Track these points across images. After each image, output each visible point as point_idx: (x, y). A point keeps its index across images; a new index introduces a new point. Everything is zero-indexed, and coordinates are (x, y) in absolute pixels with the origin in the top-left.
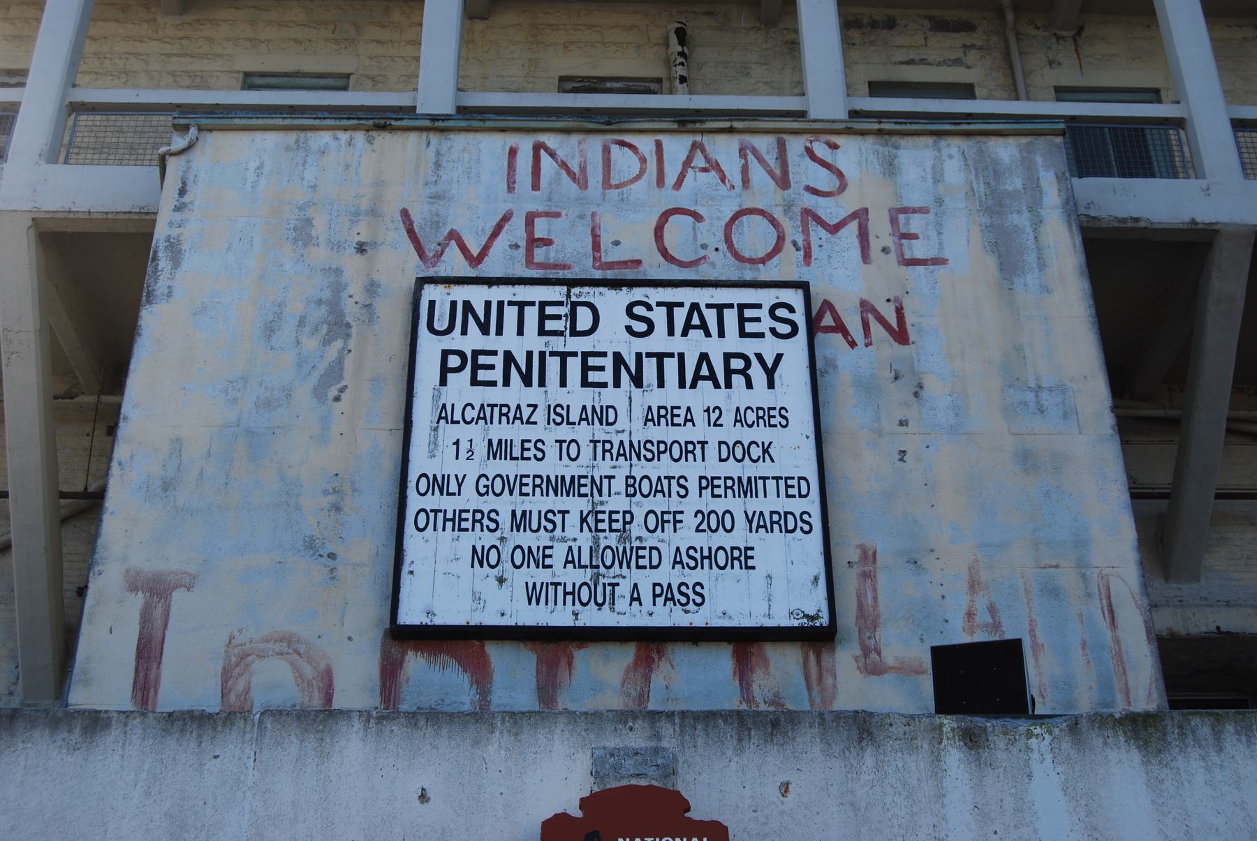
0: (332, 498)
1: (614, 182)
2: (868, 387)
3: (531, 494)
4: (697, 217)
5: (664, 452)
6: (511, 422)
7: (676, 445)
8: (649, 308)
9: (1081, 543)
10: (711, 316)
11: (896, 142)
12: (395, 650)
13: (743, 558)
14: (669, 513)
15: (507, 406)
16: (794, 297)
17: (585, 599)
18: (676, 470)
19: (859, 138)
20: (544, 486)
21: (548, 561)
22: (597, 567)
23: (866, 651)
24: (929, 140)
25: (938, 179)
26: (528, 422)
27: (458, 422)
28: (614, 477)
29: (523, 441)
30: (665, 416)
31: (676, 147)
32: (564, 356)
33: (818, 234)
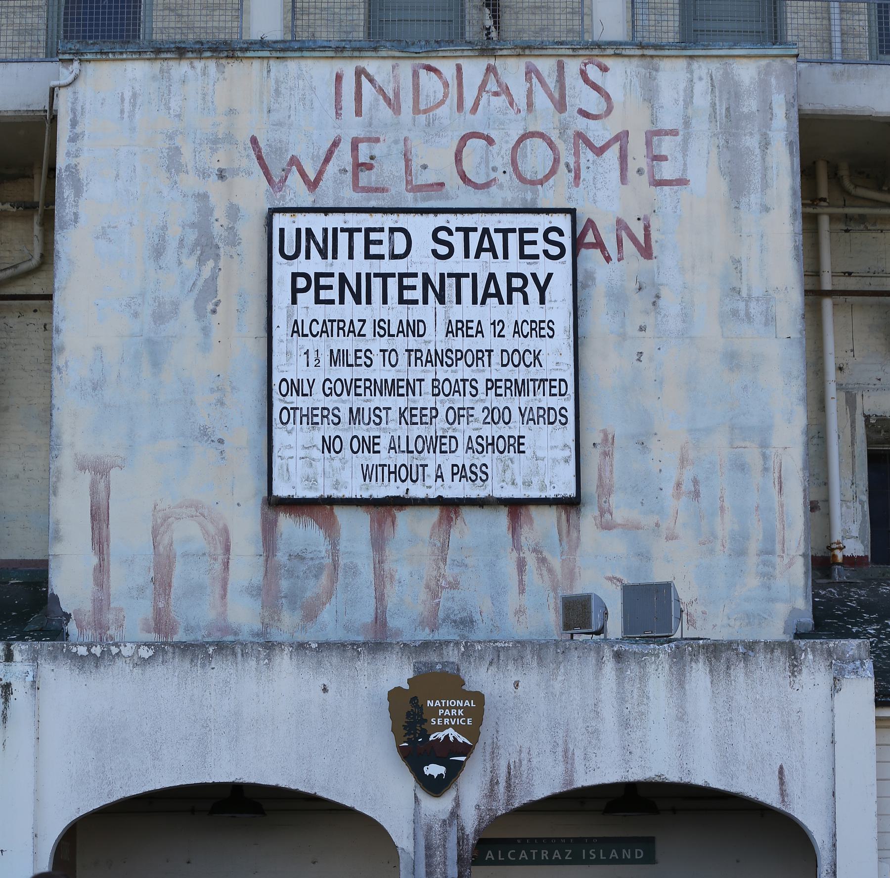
0: (217, 395)
1: (422, 107)
2: (617, 297)
3: (363, 395)
4: (490, 141)
5: (460, 359)
6: (346, 335)
8: (450, 233)
10: (498, 239)
11: (657, 64)
12: (271, 514)
13: (517, 444)
14: (464, 409)
15: (343, 321)
16: (563, 222)
18: (468, 374)
19: (626, 60)
20: (372, 388)
21: (377, 448)
22: (412, 452)
23: (602, 513)
26: (359, 335)
27: (307, 335)
28: (423, 380)
29: (356, 351)
30: (461, 329)
32: (385, 277)
33: (587, 155)
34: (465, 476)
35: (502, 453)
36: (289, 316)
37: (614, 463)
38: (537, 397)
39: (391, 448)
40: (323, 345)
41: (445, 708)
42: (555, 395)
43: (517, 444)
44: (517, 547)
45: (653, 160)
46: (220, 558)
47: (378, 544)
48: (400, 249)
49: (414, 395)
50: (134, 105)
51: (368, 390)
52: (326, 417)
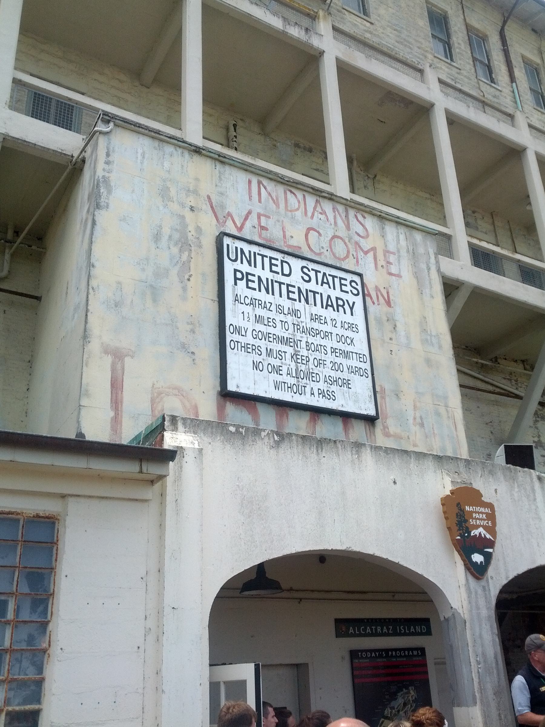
0: (191, 327)
2: (379, 321)
4: (320, 234)
5: (318, 334)
8: (309, 271)
9: (446, 398)
10: (330, 279)
13: (346, 383)
16: (357, 279)
18: (323, 342)
21: (281, 372)
24: (394, 225)
26: (269, 310)
27: (243, 304)
30: (317, 319)
31: (311, 201)
33: (361, 254)
36: (234, 292)
41: (476, 512)
43: (346, 383)
50: (144, 157)
52: (254, 350)
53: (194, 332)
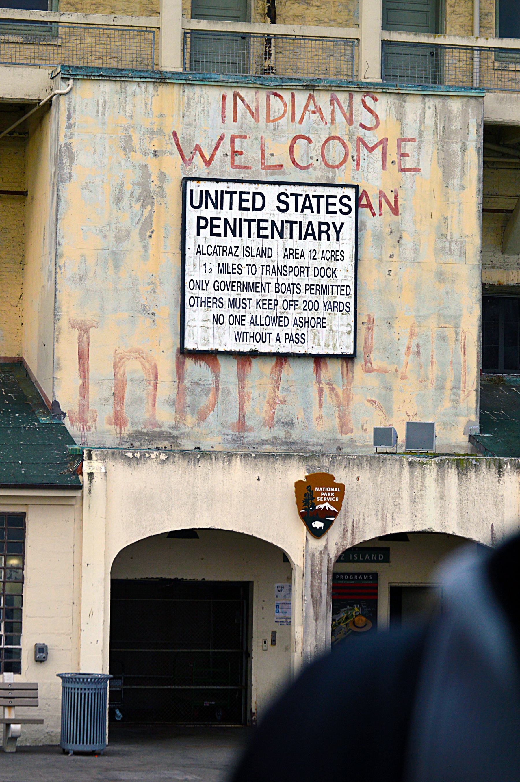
0: (151, 287)
2: (378, 237)
4: (309, 141)
5: (291, 272)
7: (296, 268)
8: (287, 197)
10: (314, 201)
12: (181, 357)
13: (321, 322)
14: (292, 301)
15: (226, 247)
16: (351, 192)
17: (258, 340)
18: (295, 280)
19: (388, 95)
20: (242, 287)
21: (243, 322)
22: (263, 325)
25: (422, 121)
26: (235, 255)
27: (205, 254)
28: (270, 283)
30: (292, 254)
31: (301, 98)
32: (250, 221)
34: (293, 340)
35: (313, 327)
37: (374, 334)
38: (333, 295)
39: (251, 323)
40: (214, 260)
41: (324, 492)
42: (344, 295)
44: (319, 381)
45: (401, 156)
46: (152, 383)
47: (241, 378)
48: (259, 205)
49: (265, 292)
50: (105, 109)
51: (239, 288)
52: (215, 303)
53: (155, 292)
